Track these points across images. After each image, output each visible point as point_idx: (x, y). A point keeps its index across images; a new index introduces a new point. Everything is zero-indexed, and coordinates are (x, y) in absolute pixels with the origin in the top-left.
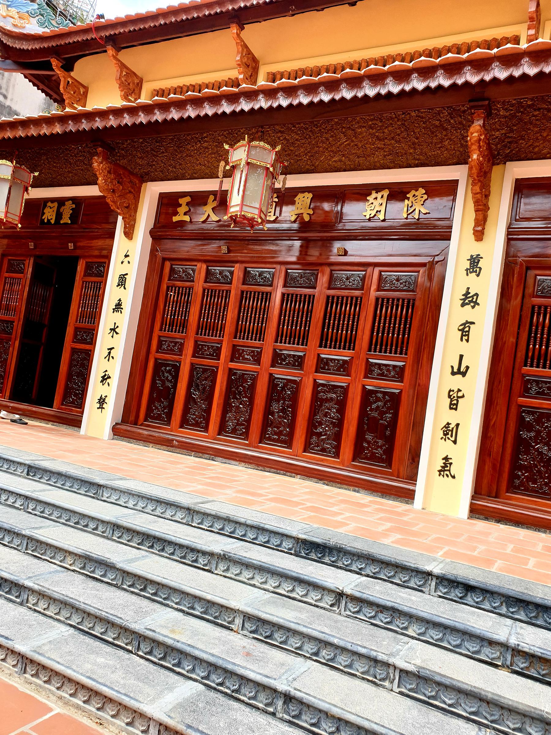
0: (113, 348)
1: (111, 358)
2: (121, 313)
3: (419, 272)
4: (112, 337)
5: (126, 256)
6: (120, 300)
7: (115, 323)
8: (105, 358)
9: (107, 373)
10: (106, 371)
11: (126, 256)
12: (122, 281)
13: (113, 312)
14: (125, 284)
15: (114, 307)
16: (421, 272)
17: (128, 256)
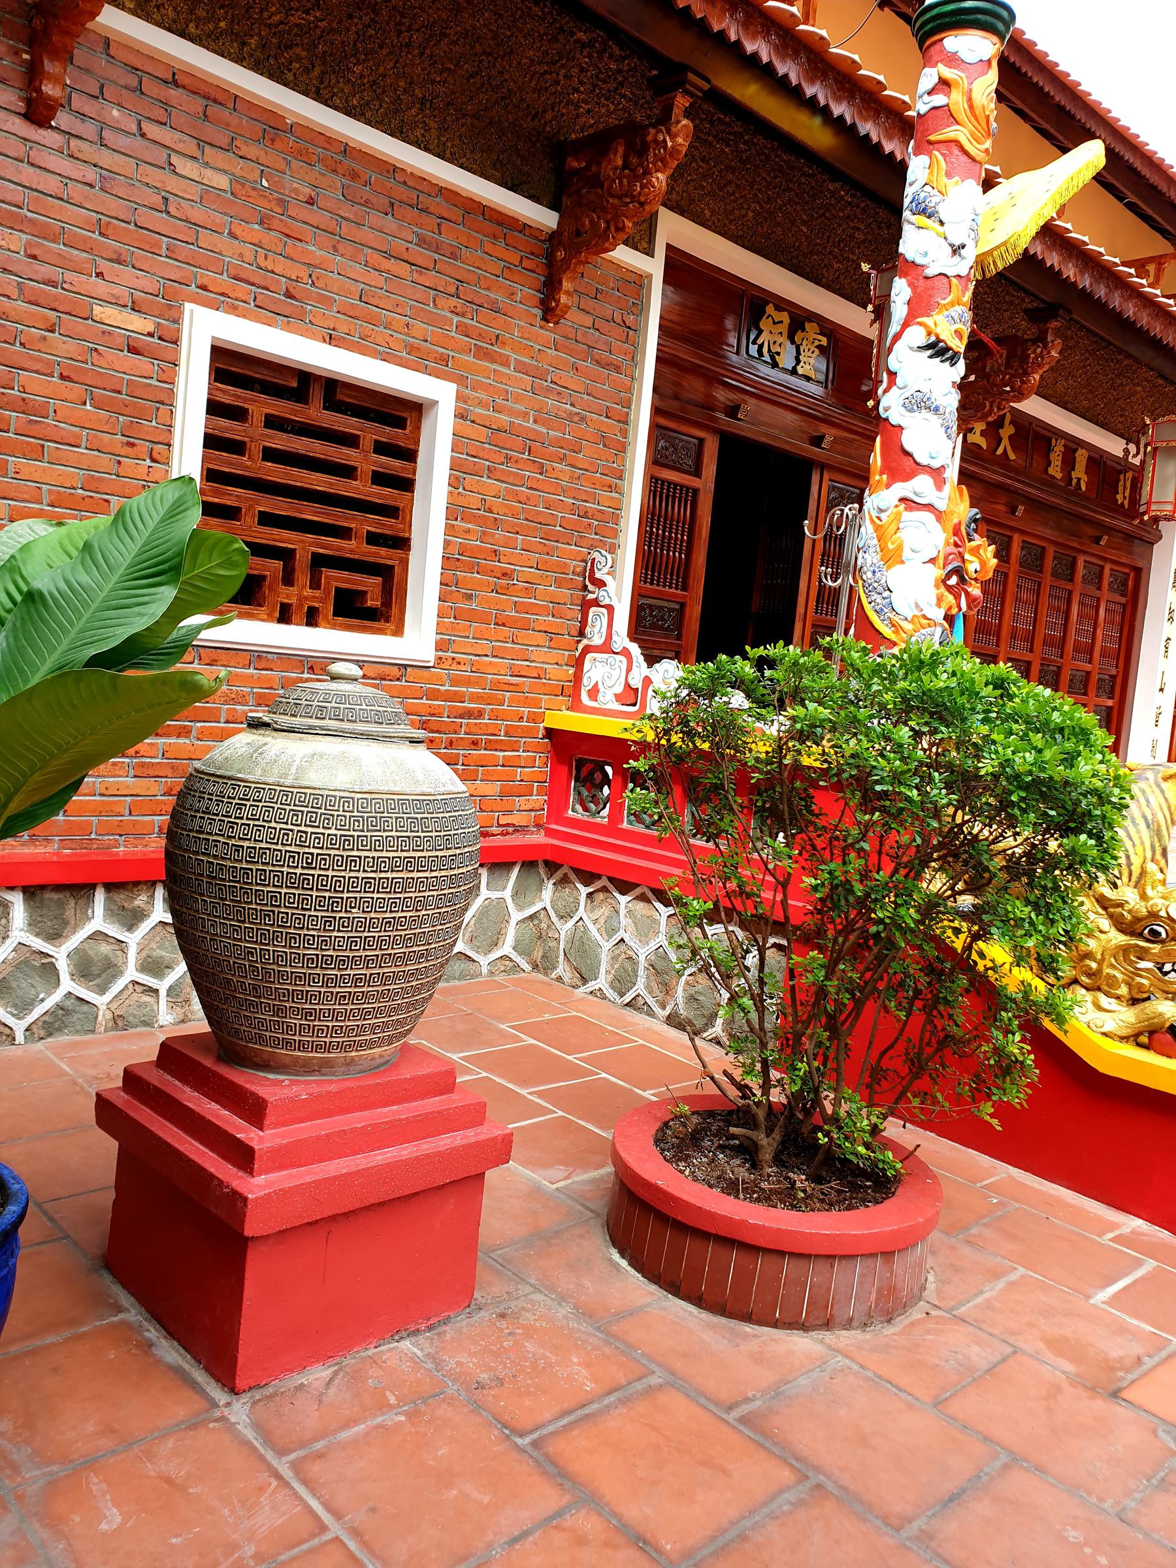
3: (1128, 575)
16: (1132, 575)
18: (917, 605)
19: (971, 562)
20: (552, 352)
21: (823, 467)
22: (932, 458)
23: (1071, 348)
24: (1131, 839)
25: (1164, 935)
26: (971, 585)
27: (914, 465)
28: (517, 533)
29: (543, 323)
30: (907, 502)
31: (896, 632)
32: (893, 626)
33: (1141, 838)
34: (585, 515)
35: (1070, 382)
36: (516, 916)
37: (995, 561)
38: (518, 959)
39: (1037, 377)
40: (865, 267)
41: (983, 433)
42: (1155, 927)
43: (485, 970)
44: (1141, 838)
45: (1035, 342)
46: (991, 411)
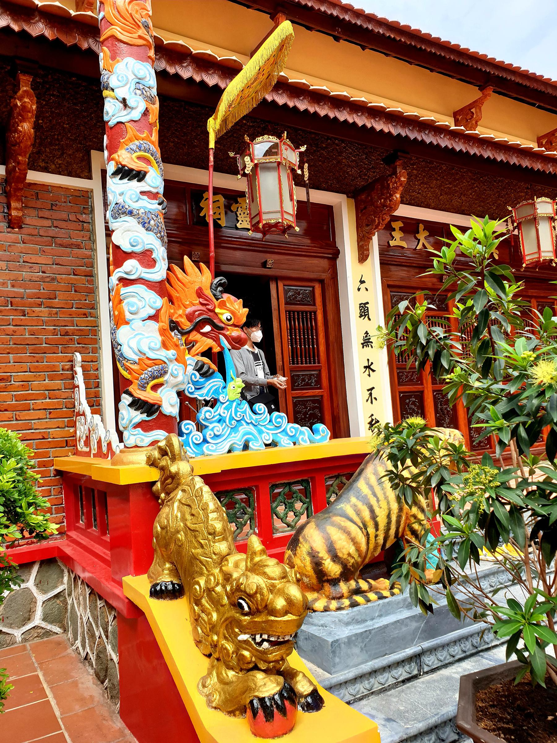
0: (373, 388)
1: (373, 400)
2: (372, 347)
4: (369, 375)
5: (362, 282)
6: (367, 333)
7: (368, 360)
8: (367, 400)
9: (373, 417)
10: (372, 415)
11: (362, 282)
12: (364, 311)
13: (363, 347)
14: (368, 314)
15: (363, 342)
17: (364, 282)
18: (140, 352)
19: (222, 314)
20: (22, 245)
21: (276, 279)
22: (133, 246)
23: (458, 180)
24: (375, 495)
25: (246, 609)
26: (228, 330)
27: (124, 255)
28: (9, 353)
29: (9, 230)
30: (125, 282)
31: (130, 373)
32: (128, 369)
33: (385, 494)
34: (67, 334)
35: (464, 198)
36: (41, 598)
37: (247, 310)
38: (49, 627)
39: (398, 196)
40: (232, 154)
41: (402, 239)
42: (241, 601)
43: (19, 639)
44: (385, 494)
45: (390, 176)
46: (379, 223)
